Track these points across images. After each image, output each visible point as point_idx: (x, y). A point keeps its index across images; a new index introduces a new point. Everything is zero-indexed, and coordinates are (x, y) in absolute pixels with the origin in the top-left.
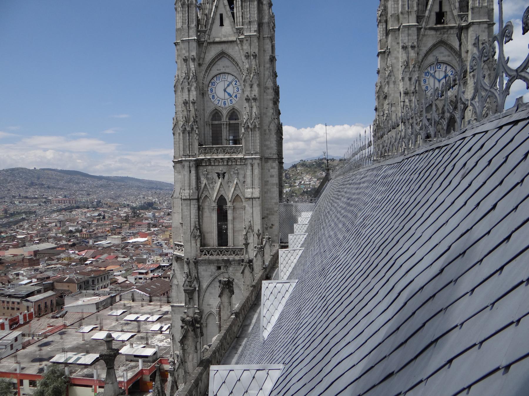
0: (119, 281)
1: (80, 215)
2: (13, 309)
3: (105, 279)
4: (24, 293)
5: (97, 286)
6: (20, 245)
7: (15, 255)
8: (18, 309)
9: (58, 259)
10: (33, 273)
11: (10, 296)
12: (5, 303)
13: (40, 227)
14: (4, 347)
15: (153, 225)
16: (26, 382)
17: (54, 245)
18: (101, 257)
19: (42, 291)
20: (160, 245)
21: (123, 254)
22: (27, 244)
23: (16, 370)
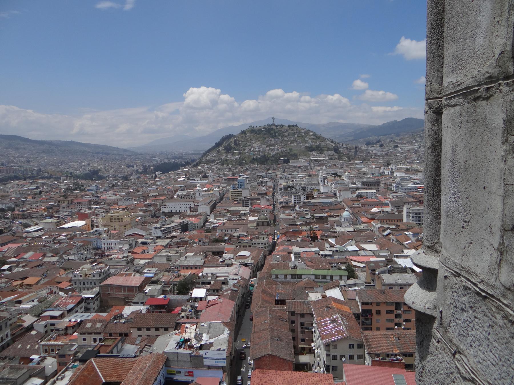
0: (26, 325)
15: (95, 202)
21: (51, 252)
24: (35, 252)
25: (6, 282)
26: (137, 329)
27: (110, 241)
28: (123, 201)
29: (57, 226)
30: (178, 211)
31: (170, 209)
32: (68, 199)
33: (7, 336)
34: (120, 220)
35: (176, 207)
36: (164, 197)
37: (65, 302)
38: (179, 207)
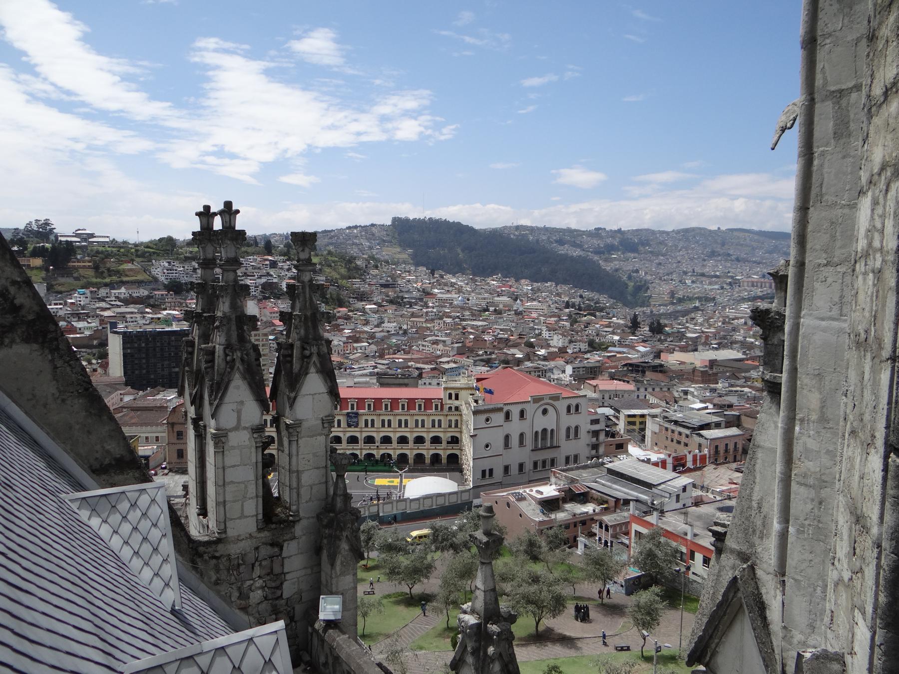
2: (679, 442)
4: (696, 421)
6: (690, 348)
7: (682, 363)
8: (686, 445)
9: (747, 379)
10: (708, 394)
11: (676, 423)
12: (670, 431)
13: (720, 324)
14: (668, 495)
16: (699, 557)
17: (740, 355)
19: (723, 425)
22: (700, 348)
23: (686, 534)
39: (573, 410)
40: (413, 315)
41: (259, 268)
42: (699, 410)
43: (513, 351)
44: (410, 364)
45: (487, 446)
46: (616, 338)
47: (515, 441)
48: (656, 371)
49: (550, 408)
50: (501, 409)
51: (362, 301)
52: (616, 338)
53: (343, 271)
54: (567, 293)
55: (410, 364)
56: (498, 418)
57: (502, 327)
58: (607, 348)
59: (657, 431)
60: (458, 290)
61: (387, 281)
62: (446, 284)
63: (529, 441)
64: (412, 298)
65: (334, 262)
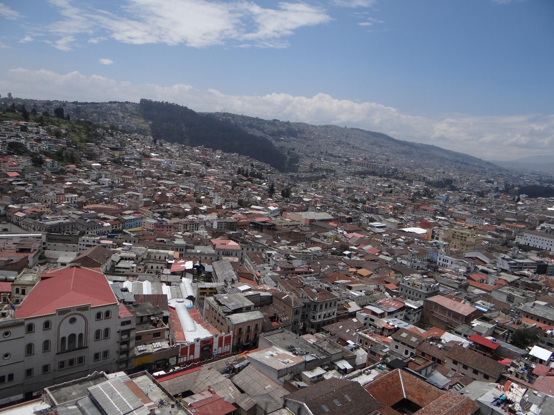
0: (350, 310)
1: (369, 185)
3: (330, 306)
5: (319, 314)
9: (325, 237)
15: (441, 213)
17: (330, 217)
18: (364, 248)
20: (437, 246)
22: (310, 208)
24: (374, 247)
25: (344, 266)
26: (452, 362)
27: (446, 257)
28: (472, 219)
29: (399, 227)
30: (538, 247)
31: (527, 242)
32: (415, 204)
33: (334, 314)
34: (463, 239)
35: (536, 241)
36: (523, 226)
37: (388, 303)
38: (540, 242)
39: (103, 316)
40: (125, 173)
41: (11, 131)
42: (244, 291)
43: (183, 206)
44: (99, 215)
45: (6, 355)
46: (259, 198)
47: (38, 348)
48: (270, 229)
49: (77, 317)
50: (22, 324)
51: (91, 159)
52: (259, 198)
53: (84, 136)
54: (244, 163)
55: (99, 215)
56: (22, 330)
57: (185, 187)
58: (251, 205)
59: (208, 309)
60: (168, 156)
61: (117, 146)
62: (162, 150)
63: (54, 347)
64: (132, 159)
65: (79, 129)
